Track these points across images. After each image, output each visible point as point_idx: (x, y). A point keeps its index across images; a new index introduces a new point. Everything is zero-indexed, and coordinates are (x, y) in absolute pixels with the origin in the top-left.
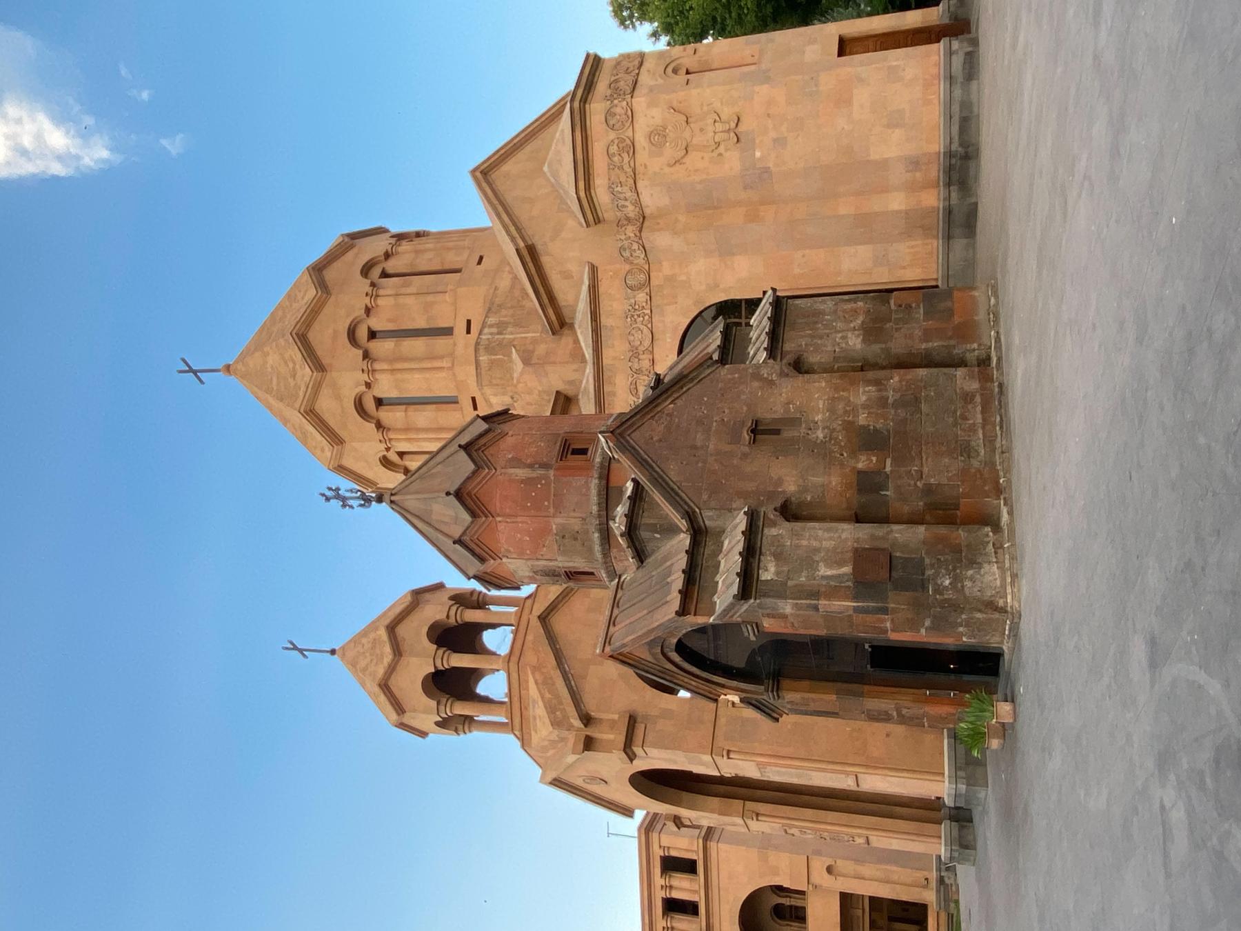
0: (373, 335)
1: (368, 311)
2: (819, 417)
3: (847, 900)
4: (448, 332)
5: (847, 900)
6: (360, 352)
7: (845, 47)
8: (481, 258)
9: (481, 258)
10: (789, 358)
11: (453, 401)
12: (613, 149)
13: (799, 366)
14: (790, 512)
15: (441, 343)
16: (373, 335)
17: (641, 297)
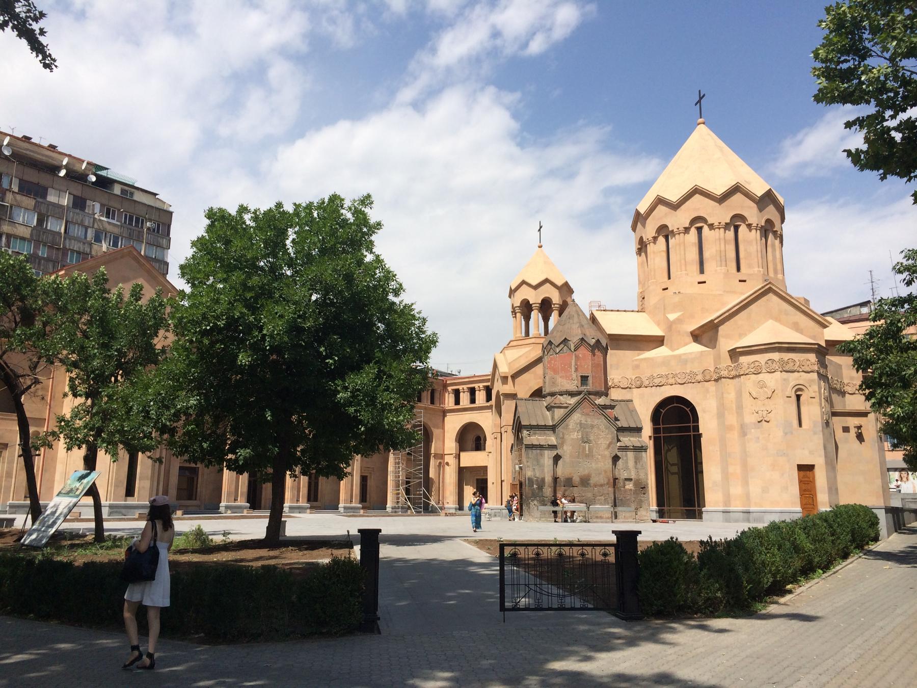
0: (699, 230)
1: (711, 227)
2: (593, 465)
3: (485, 468)
4: (702, 271)
5: (485, 468)
6: (687, 225)
7: (806, 469)
8: (745, 281)
9: (745, 281)
10: (619, 454)
11: (669, 278)
12: (757, 364)
13: (616, 459)
14: (557, 458)
15: (696, 267)
16: (699, 230)
17: (699, 378)
